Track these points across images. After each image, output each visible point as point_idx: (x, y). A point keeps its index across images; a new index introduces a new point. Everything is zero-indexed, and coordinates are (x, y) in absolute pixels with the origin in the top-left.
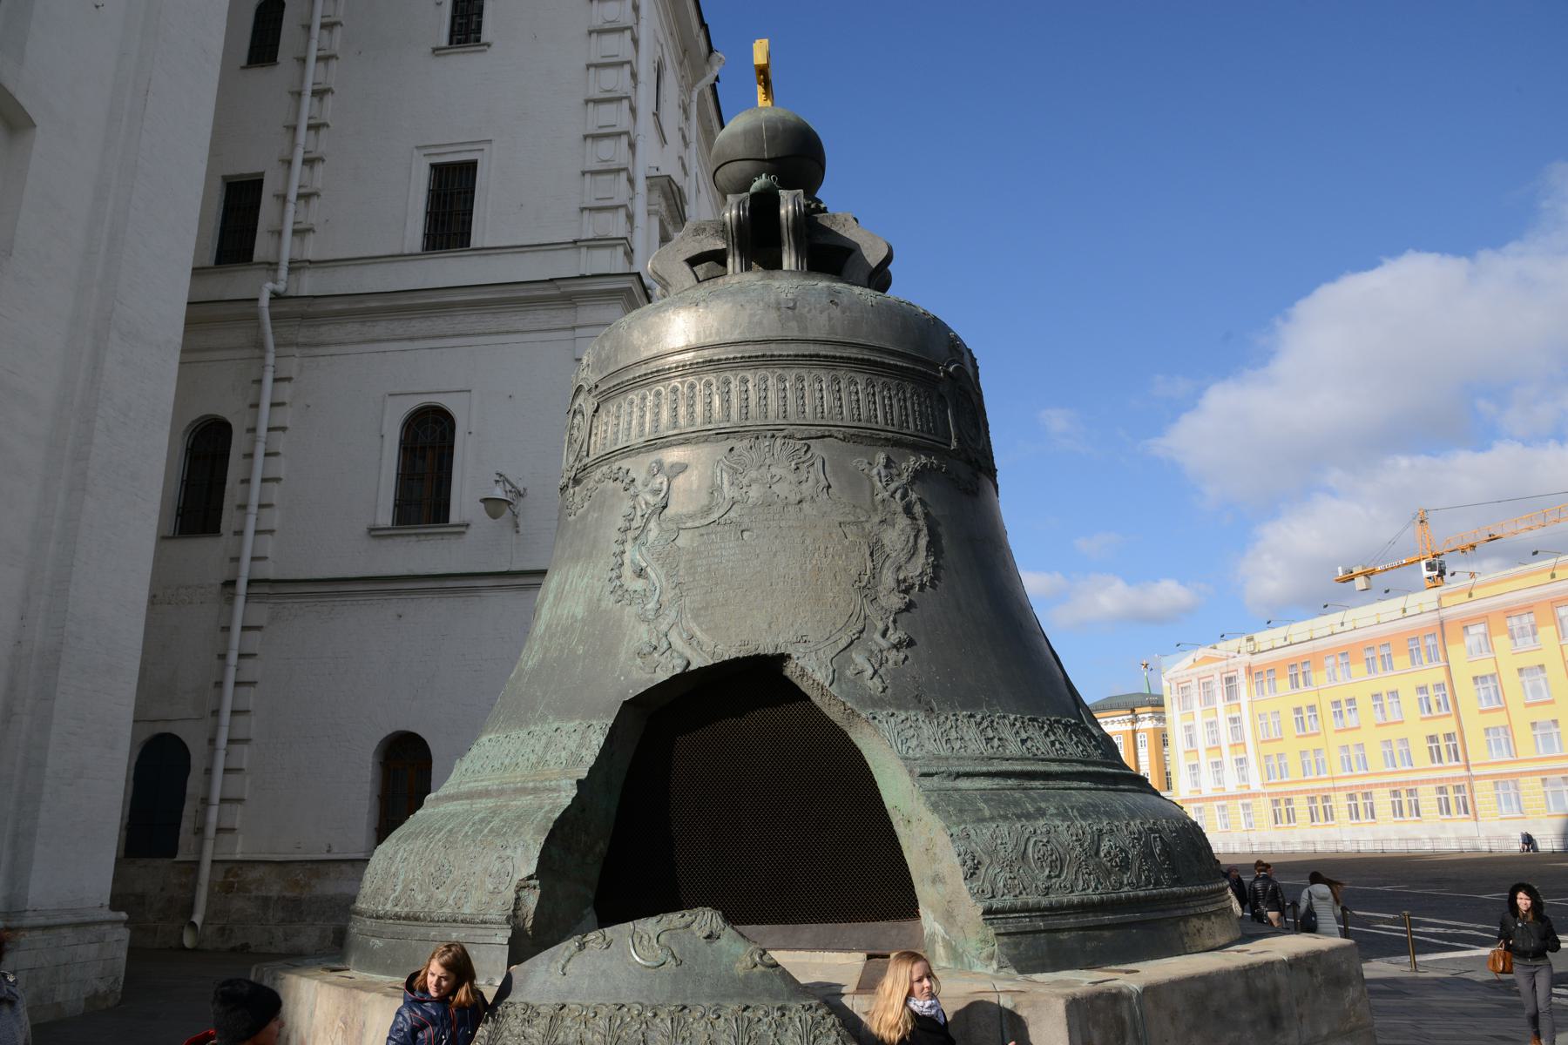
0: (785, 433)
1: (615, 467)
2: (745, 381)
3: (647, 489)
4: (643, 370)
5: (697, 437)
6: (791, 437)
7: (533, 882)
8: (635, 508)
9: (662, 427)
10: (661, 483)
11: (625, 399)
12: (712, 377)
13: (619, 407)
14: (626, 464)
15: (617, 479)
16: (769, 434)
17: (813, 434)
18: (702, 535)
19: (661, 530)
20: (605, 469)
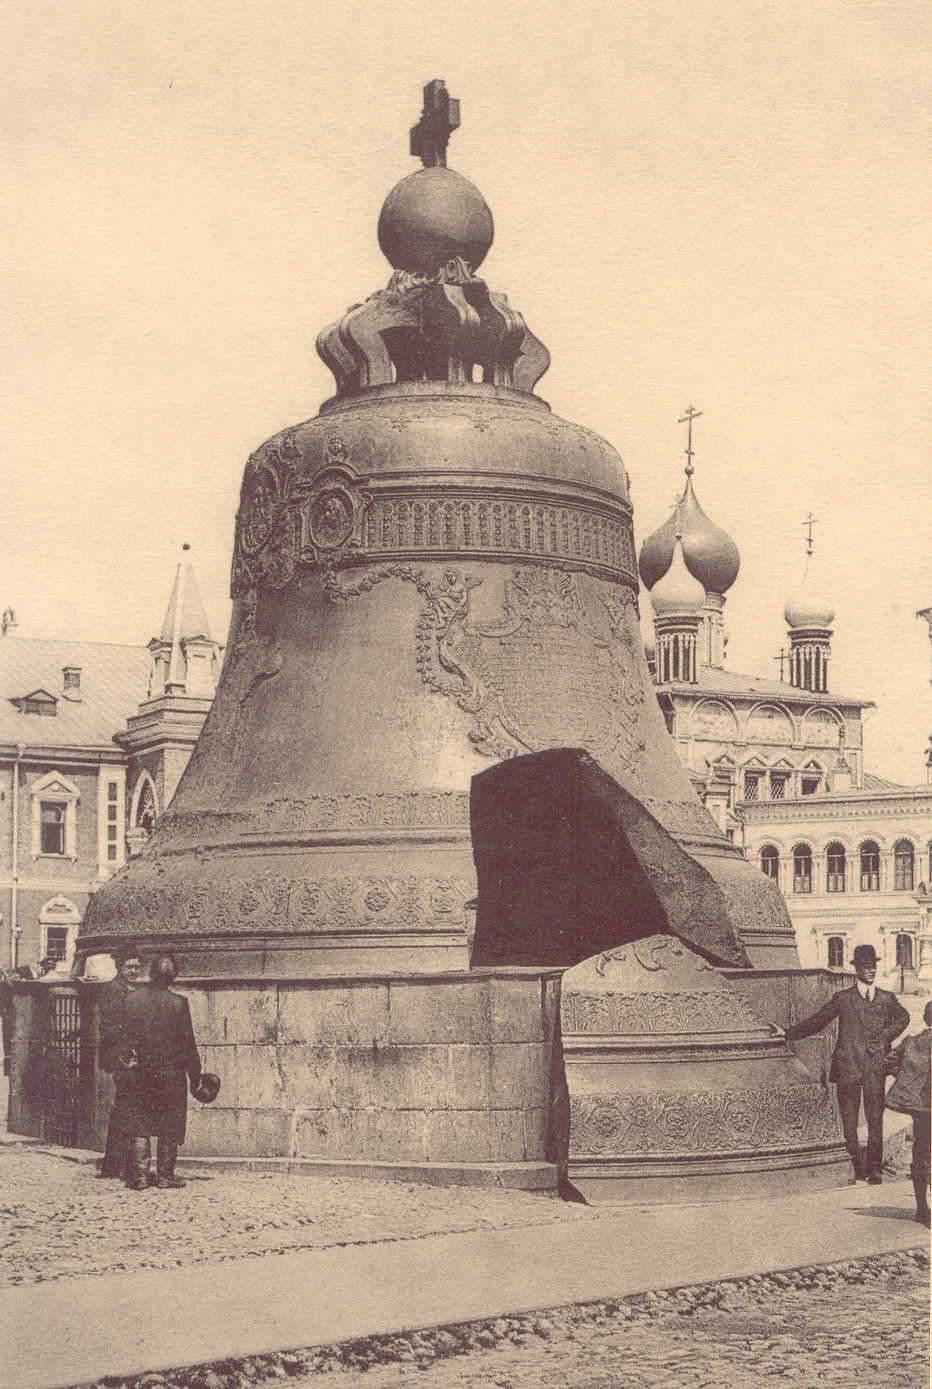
0: (555, 564)
1: (406, 567)
2: (526, 512)
3: (444, 594)
4: (430, 481)
5: (491, 556)
6: (562, 570)
7: (473, 906)
8: (436, 610)
9: (456, 542)
10: (461, 592)
11: (411, 504)
12: (500, 503)
13: (403, 509)
14: (415, 567)
15: (409, 578)
16: (545, 563)
17: (575, 567)
18: (502, 644)
19: (467, 635)
20: (389, 565)
